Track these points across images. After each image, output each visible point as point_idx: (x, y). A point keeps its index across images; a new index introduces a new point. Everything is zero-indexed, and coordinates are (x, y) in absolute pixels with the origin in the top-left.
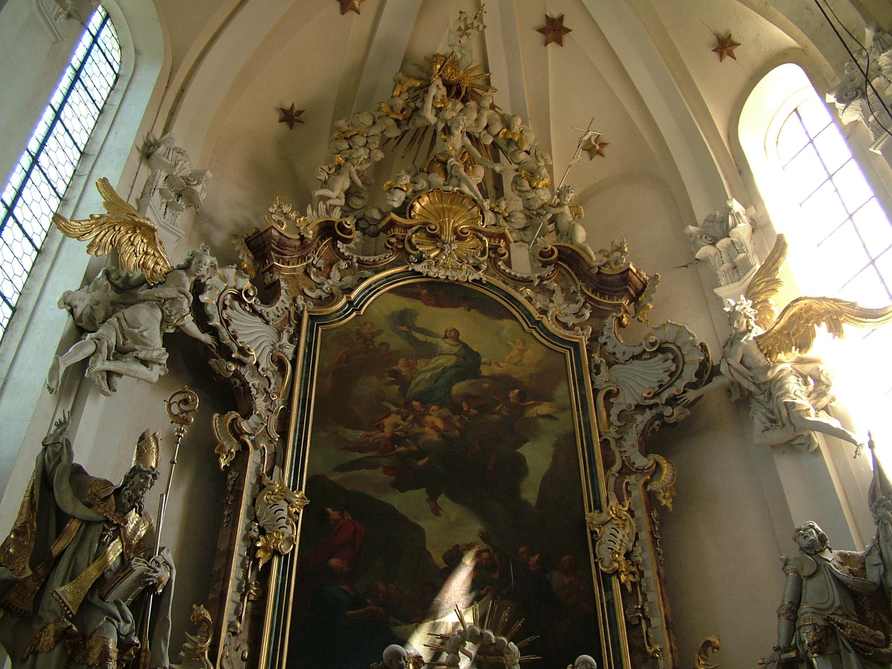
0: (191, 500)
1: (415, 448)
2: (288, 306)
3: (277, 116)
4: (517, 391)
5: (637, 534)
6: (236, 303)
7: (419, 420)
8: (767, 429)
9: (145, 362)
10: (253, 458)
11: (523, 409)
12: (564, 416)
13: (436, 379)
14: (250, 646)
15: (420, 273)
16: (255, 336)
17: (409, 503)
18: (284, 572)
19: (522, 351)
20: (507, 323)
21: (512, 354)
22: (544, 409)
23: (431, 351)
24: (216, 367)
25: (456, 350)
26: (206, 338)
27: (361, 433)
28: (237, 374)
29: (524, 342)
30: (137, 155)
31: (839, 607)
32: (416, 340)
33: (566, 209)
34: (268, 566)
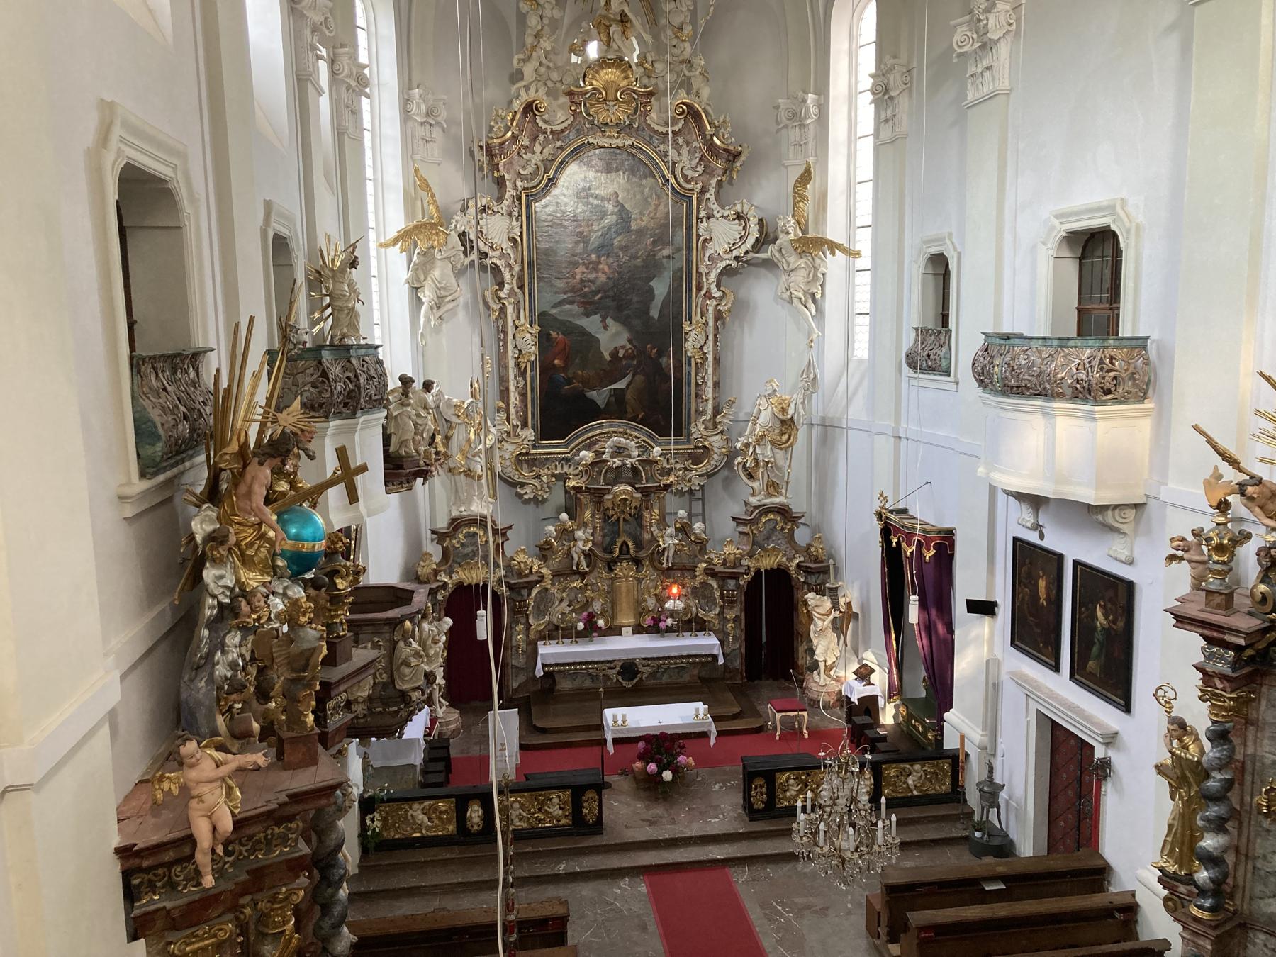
10: (510, 309)
17: (591, 324)
19: (657, 206)
20: (650, 180)
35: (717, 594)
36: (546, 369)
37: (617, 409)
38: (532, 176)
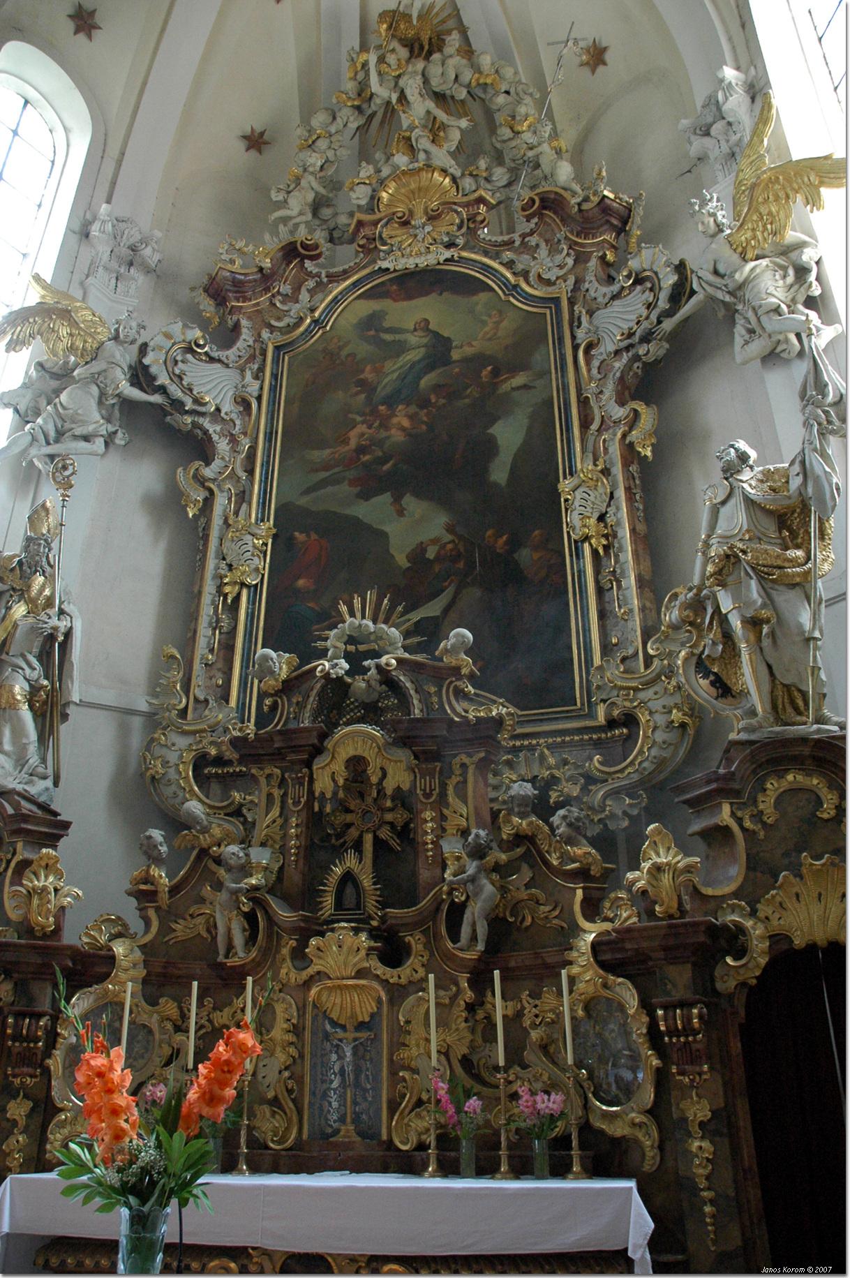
0: (170, 553)
1: (380, 454)
2: (251, 343)
3: (242, 145)
4: (489, 368)
5: (612, 493)
6: (189, 356)
7: (384, 426)
8: (747, 343)
9: (86, 438)
10: (220, 502)
11: (495, 386)
12: (539, 383)
13: (402, 378)
14: (224, 673)
15: (388, 269)
18: (252, 602)
19: (498, 323)
20: (483, 297)
21: (487, 329)
22: (519, 380)
23: (400, 348)
24: (173, 423)
25: (425, 340)
26: (156, 398)
27: (328, 451)
28: (194, 424)
29: (500, 312)
30: (74, 239)
31: (748, 531)
32: (384, 341)
33: (545, 147)
34: (237, 598)
35: (639, 1028)
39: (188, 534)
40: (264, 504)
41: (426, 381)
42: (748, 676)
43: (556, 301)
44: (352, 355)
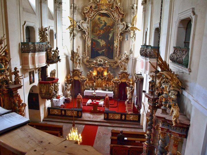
7: (100, 32)
10: (87, 38)
16: (85, 26)
17: (99, 40)
20: (110, 18)
22: (112, 30)
23: (102, 23)
36: (92, 47)
37: (103, 54)
38: (91, 18)
39: (84, 42)
40: (90, 38)
41: (104, 28)
42: (123, 66)
43: (116, 21)
44: (97, 23)
